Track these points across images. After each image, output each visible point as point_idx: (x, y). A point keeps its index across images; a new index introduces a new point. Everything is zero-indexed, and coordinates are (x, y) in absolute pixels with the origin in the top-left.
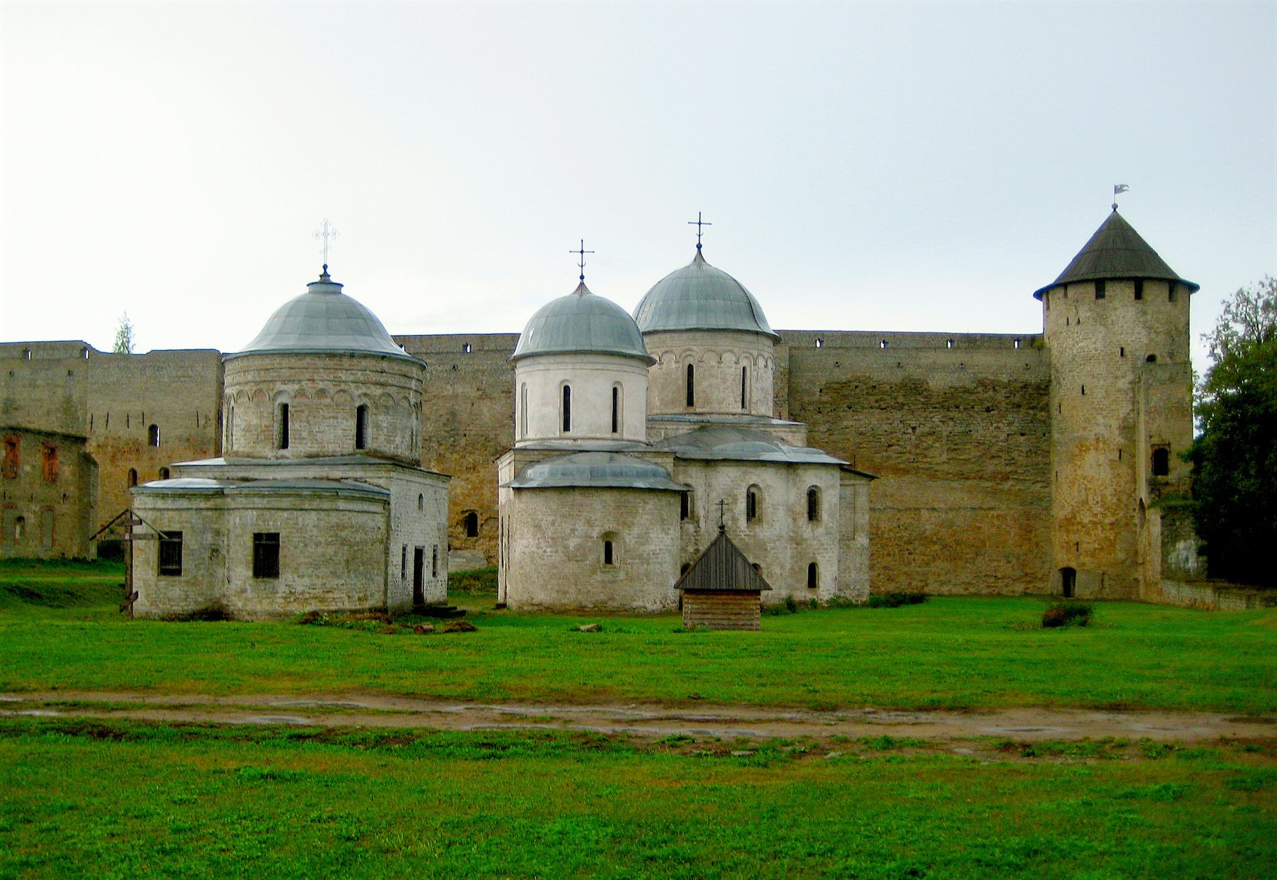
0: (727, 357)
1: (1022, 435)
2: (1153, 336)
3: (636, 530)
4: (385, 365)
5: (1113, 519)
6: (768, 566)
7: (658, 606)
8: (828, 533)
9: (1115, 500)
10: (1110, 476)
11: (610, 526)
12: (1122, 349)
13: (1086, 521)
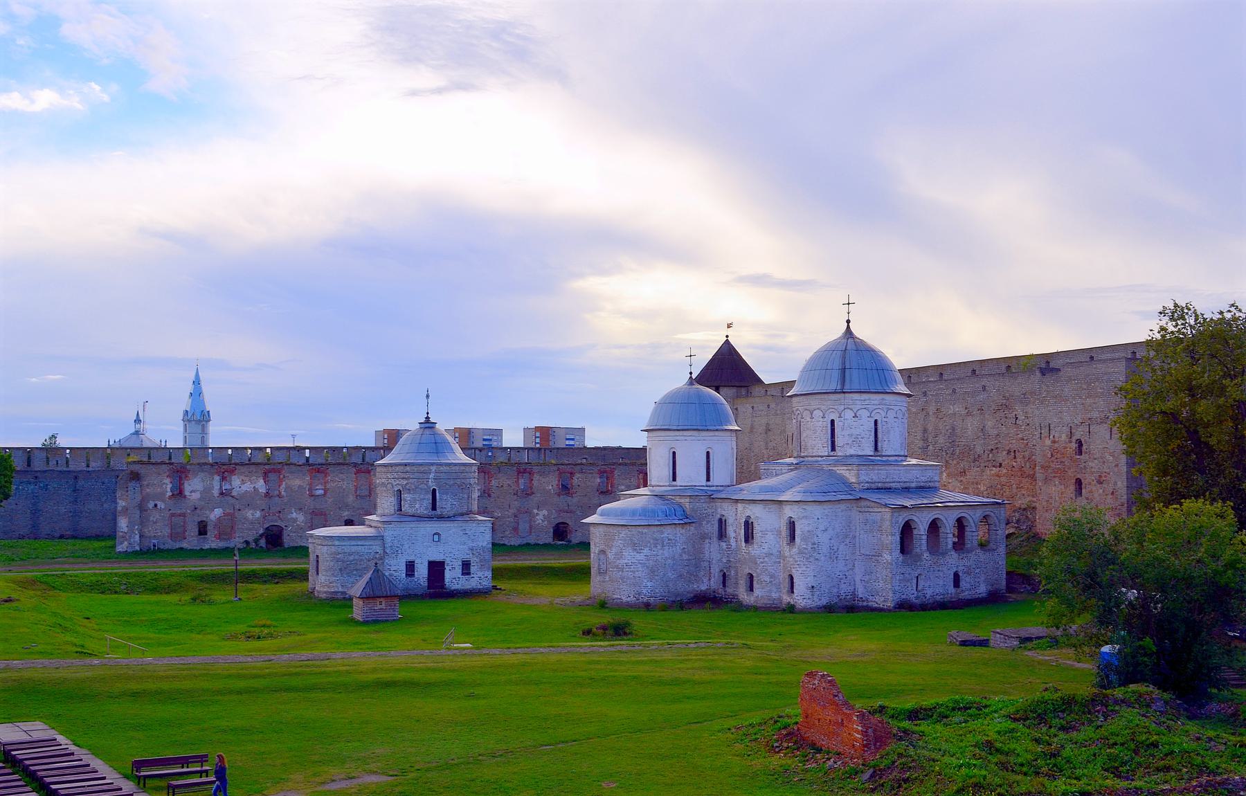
0: (817, 413)
3: (614, 550)
4: (408, 468)
7: (632, 599)
8: (800, 552)
11: (602, 547)
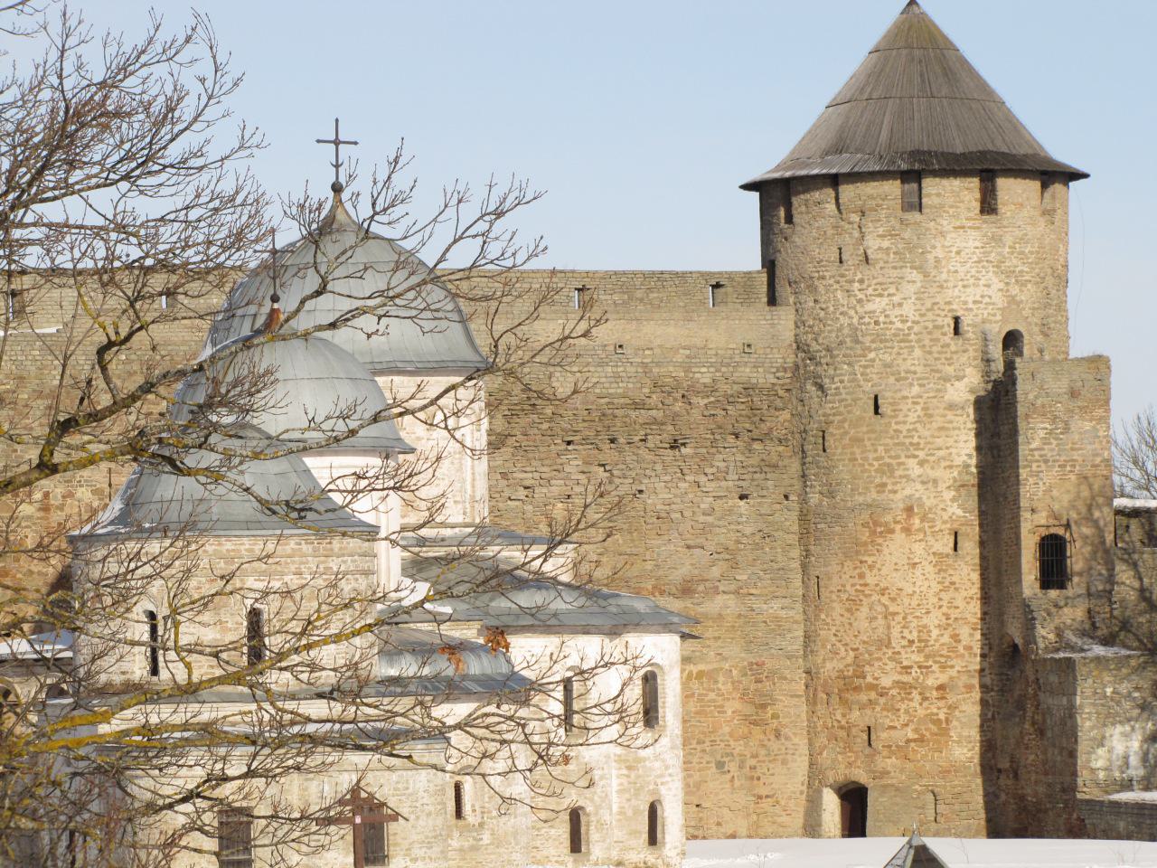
1: (742, 497)
2: (1015, 290)
5: (943, 678)
6: (598, 808)
9: (946, 639)
10: (936, 587)
12: (957, 320)
13: (886, 682)
